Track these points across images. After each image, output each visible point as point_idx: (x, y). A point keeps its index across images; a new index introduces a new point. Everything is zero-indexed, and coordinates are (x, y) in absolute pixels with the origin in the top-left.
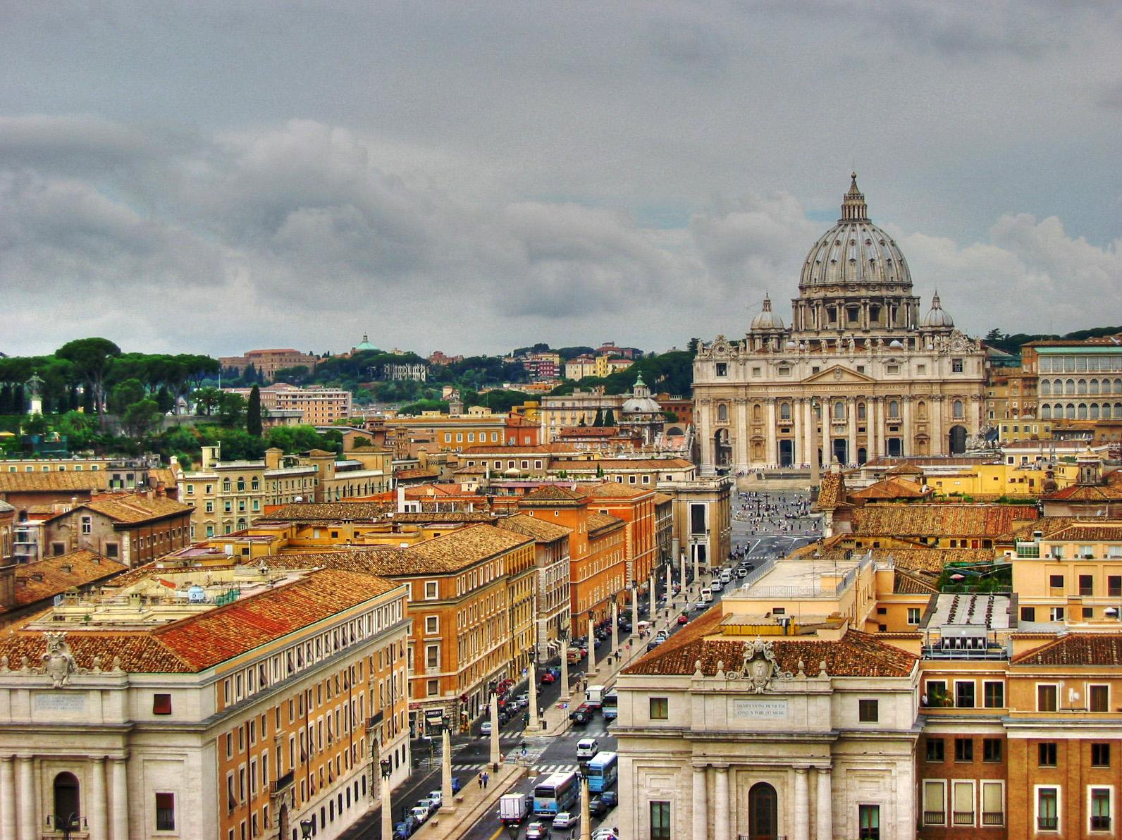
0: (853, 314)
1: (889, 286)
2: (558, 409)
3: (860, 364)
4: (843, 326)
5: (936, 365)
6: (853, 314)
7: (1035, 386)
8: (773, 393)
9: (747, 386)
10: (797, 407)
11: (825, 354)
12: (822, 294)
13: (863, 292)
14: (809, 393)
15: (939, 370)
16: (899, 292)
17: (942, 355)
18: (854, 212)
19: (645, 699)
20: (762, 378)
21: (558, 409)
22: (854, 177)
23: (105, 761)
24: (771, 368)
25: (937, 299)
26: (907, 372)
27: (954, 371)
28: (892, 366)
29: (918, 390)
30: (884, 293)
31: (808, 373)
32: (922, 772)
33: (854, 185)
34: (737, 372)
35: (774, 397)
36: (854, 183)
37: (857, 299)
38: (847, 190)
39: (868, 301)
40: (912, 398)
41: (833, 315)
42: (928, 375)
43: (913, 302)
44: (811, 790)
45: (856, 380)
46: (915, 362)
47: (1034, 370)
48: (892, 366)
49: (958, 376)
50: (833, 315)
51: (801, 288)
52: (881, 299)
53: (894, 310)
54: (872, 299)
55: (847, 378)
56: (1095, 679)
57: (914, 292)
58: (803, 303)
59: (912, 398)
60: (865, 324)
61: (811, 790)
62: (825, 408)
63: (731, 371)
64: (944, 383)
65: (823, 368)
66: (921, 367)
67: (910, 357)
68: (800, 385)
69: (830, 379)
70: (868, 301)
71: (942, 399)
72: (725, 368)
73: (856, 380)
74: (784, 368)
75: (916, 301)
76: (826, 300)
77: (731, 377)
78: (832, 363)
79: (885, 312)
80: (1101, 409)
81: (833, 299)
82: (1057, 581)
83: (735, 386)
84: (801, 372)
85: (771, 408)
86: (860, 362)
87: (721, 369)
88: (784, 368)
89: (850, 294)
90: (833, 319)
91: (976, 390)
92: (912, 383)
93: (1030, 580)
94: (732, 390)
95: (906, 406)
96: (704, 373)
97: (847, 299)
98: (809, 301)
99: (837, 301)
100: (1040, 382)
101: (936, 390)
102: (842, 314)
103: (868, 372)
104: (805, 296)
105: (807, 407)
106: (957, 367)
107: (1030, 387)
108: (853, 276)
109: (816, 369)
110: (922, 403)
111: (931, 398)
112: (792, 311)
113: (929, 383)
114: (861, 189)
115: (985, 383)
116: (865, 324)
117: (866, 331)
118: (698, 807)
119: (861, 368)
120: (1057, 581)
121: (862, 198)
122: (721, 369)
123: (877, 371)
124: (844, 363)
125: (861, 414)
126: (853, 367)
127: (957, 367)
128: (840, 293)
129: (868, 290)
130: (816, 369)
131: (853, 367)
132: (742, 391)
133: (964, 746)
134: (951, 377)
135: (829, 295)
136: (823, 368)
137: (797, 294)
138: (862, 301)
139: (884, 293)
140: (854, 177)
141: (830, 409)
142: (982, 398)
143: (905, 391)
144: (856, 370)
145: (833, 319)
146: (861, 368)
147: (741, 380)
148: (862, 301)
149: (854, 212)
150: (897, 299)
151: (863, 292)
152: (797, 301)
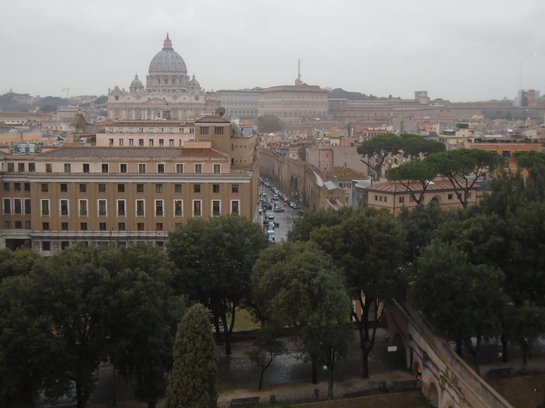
0: (166, 81)
1: (179, 72)
2: (63, 111)
6: (166, 81)
8: (134, 106)
9: (126, 104)
10: (143, 111)
11: (152, 93)
12: (156, 74)
13: (170, 74)
14: (147, 107)
15: (192, 99)
16: (182, 74)
17: (192, 94)
20: (131, 101)
21: (63, 111)
24: (134, 98)
25: (194, 76)
26: (180, 99)
27: (196, 100)
28: (175, 98)
29: (184, 106)
30: (177, 74)
31: (146, 100)
33: (168, 36)
36: (168, 36)
38: (165, 38)
40: (181, 109)
41: (159, 81)
43: (188, 77)
45: (163, 103)
46: (182, 97)
48: (175, 98)
50: (159, 81)
51: (150, 72)
52: (175, 76)
53: (180, 81)
54: (173, 76)
55: (159, 102)
56: (66, 161)
57: (188, 75)
62: (152, 112)
63: (120, 99)
64: (192, 104)
65: (152, 98)
66: (185, 98)
67: (181, 95)
68: (143, 103)
69: (153, 102)
71: (191, 109)
73: (163, 103)
74: (138, 97)
76: (157, 76)
77: (120, 100)
78: (154, 96)
79: (177, 81)
80: (242, 113)
81: (159, 76)
83: (121, 104)
84: (144, 99)
85: (134, 112)
86: (164, 96)
87: (117, 98)
88: (138, 97)
89: (165, 74)
91: (203, 107)
92: (182, 104)
96: (112, 100)
98: (152, 76)
101: (190, 107)
102: (162, 81)
105: (146, 112)
106: (197, 99)
109: (149, 99)
111: (188, 109)
112: (146, 79)
113: (187, 104)
114: (170, 38)
117: (170, 87)
119: (164, 99)
122: (117, 98)
123: (169, 99)
124: (159, 97)
126: (162, 98)
127: (197, 99)
128: (162, 74)
130: (149, 99)
131: (162, 98)
132: (124, 106)
133: (17, 185)
135: (158, 74)
136: (152, 98)
137: (148, 74)
139: (177, 74)
143: (179, 107)
146: (164, 99)
147: (123, 101)
149: (168, 46)
150: (182, 76)
151: (170, 74)
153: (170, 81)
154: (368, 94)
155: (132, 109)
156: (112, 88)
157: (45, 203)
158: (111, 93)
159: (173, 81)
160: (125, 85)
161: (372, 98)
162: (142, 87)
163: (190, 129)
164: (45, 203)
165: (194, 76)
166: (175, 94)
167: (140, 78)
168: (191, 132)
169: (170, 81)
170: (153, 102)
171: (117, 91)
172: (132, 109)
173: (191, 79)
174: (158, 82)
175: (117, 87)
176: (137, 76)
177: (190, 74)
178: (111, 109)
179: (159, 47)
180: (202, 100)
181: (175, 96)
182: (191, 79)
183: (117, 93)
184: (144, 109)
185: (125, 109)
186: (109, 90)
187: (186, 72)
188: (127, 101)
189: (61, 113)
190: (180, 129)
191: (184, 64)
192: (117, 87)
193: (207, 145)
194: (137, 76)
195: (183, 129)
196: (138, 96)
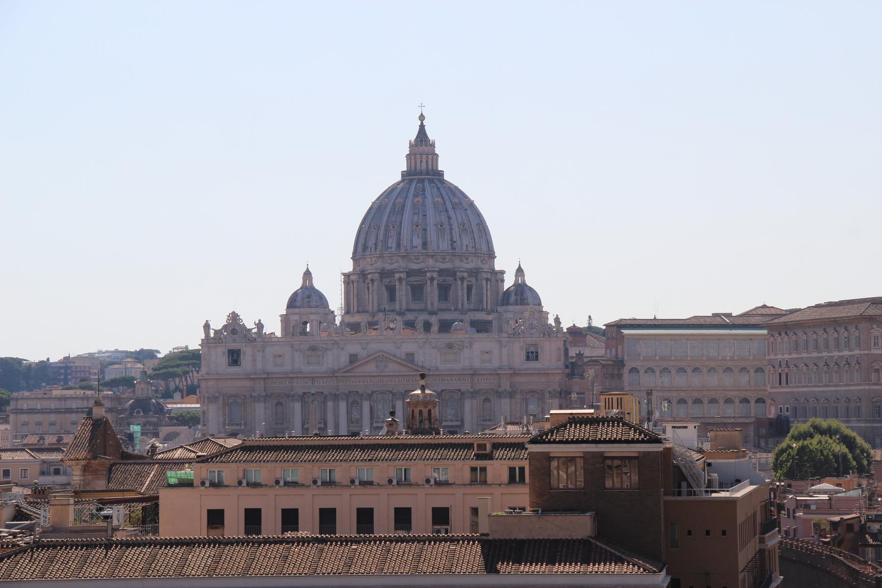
0: (417, 291)
2: (31, 411)
3: (410, 350)
4: (404, 307)
5: (505, 351)
7: (620, 376)
8: (299, 387)
9: (267, 377)
10: (330, 404)
20: (287, 367)
21: (31, 411)
22: (422, 118)
25: (520, 271)
27: (528, 358)
29: (483, 384)
31: (344, 360)
33: (422, 127)
34: (254, 361)
35: (301, 392)
36: (422, 127)
37: (421, 272)
38: (413, 135)
39: (435, 275)
40: (475, 394)
42: (496, 363)
47: (620, 356)
49: (532, 365)
52: (452, 273)
53: (469, 289)
54: (441, 272)
55: (393, 368)
57: (497, 267)
58: (352, 277)
59: (475, 394)
60: (432, 304)
62: (366, 405)
64: (515, 373)
67: (471, 344)
68: (332, 374)
70: (435, 275)
71: (511, 395)
72: (239, 355)
75: (499, 276)
76: (384, 274)
79: (459, 291)
81: (391, 273)
84: (334, 360)
85: (297, 406)
86: (409, 347)
87: (234, 357)
89: (415, 267)
90: (392, 299)
92: (474, 373)
94: (247, 383)
95: (468, 404)
97: (410, 273)
99: (397, 276)
100: (626, 370)
101: (505, 385)
102: (403, 293)
103: (420, 359)
104: (358, 269)
105: (343, 405)
106: (532, 355)
107: (612, 376)
109: (353, 358)
110: (487, 400)
111: (499, 394)
113: (495, 373)
115: (570, 376)
116: (432, 304)
117: (432, 313)
119: (410, 357)
120: (216, 518)
121: (433, 145)
122: (234, 357)
124: (389, 347)
127: (532, 355)
128: (401, 264)
129: (437, 261)
130: (353, 358)
134: (525, 367)
135: (388, 267)
137: (349, 267)
138: (429, 275)
139: (457, 263)
140: (422, 118)
141: (371, 408)
143: (466, 386)
144: (404, 357)
145: (392, 299)
146: (410, 357)
148: (429, 275)
150: (475, 273)
151: (431, 262)
152: (347, 276)
153: (432, 293)
155: (291, 397)
156: (218, 323)
158: (211, 341)
159: (444, 291)
160: (267, 314)
163: (512, 470)
165: (520, 271)
166: (446, 338)
167: (318, 284)
168: (512, 480)
169: (432, 293)
170: (371, 368)
171: (234, 332)
172: (291, 397)
173: (509, 282)
174: (385, 294)
175: (234, 317)
176: (308, 275)
177: (505, 262)
178: (212, 399)
180: (551, 356)
181: (450, 346)
182: (509, 282)
183: (234, 340)
184: (336, 397)
185: (267, 397)
186: (207, 327)
187: (491, 255)
188: (270, 368)
189: (24, 418)
190: (474, 469)
192: (234, 317)
193: (579, 526)
194: (308, 275)
195: (484, 470)
196: (313, 349)
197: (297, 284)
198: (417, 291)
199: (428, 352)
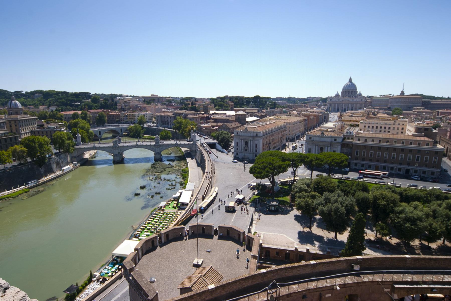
0: (349, 93)
18: (350, 80)
19: (309, 137)
23: (251, 140)
28: (353, 100)
32: (341, 148)
44: (328, 148)
48: (353, 100)
61: (328, 148)
79: (353, 93)
82: (365, 126)
87: (331, 100)
88: (339, 100)
93: (362, 126)
102: (347, 94)
106: (362, 100)
108: (349, 89)
118: (314, 149)
120: (365, 126)
122: (331, 100)
123: (351, 100)
125: (348, 106)
127: (362, 100)
142: (365, 104)
149: (350, 80)
153: (350, 93)
154: (436, 96)
157: (357, 152)
159: (351, 93)
161: (442, 98)
162: (339, 96)
164: (357, 152)
169: (350, 93)
173: (358, 93)
177: (358, 91)
179: (346, 82)
180: (364, 100)
183: (331, 98)
191: (356, 87)
197: (336, 93)
198: (349, 93)
199: (350, 100)
